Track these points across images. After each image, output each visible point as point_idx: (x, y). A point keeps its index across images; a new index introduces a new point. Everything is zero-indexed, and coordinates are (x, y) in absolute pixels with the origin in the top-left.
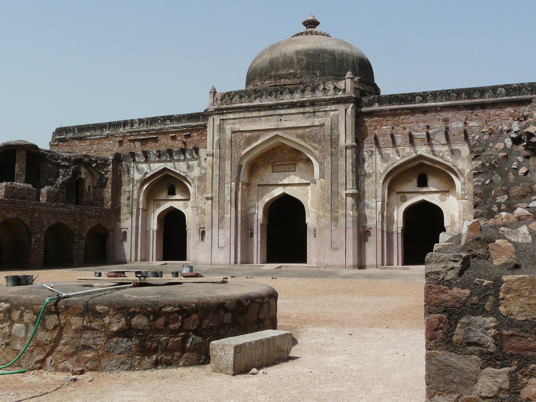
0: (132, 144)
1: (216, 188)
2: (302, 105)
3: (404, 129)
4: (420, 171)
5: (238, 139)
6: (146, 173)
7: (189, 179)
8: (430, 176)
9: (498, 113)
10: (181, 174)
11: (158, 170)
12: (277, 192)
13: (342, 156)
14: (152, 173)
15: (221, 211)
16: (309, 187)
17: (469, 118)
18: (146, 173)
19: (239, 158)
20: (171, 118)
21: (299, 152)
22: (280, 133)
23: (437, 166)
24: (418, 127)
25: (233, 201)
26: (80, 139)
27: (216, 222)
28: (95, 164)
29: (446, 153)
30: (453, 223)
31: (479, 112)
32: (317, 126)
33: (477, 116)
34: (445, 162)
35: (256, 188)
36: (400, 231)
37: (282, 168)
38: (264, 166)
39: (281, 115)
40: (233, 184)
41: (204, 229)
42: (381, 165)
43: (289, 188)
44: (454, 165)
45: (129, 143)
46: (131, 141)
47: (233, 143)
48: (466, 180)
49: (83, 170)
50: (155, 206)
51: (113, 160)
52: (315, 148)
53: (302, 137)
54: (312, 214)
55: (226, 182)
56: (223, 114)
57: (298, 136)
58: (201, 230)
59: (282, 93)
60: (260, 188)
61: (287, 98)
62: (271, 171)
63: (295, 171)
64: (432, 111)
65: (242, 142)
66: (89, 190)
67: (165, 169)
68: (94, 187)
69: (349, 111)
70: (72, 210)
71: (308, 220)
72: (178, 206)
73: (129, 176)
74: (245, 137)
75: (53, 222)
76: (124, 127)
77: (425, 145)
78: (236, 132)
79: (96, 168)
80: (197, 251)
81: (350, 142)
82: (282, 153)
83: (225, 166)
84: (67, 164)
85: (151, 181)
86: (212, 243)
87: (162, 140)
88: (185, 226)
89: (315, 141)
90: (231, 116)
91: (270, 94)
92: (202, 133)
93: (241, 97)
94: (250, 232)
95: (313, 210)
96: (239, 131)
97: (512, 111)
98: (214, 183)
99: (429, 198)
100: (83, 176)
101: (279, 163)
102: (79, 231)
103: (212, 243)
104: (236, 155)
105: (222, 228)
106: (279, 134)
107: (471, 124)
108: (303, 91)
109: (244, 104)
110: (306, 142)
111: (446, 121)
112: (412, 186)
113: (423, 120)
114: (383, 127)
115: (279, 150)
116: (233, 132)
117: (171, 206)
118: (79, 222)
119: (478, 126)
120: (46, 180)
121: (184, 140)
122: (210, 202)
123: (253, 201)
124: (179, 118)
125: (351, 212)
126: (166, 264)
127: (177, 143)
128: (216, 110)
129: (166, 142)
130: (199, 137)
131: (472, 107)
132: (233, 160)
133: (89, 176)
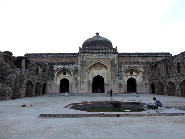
1: (81, 73)
2: (105, 53)
3: (128, 61)
6: (58, 68)
12: (97, 75)
16: (105, 74)
18: (58, 68)
20: (66, 54)
21: (103, 65)
22: (99, 60)
26: (34, 57)
30: (139, 83)
31: (145, 58)
35: (91, 73)
36: (126, 85)
39: (100, 55)
49: (39, 67)
52: (108, 64)
53: (105, 62)
56: (83, 54)
57: (104, 61)
59: (100, 50)
61: (101, 51)
69: (117, 56)
71: (105, 82)
72: (67, 78)
75: (37, 82)
76: (50, 55)
84: (35, 64)
90: (86, 54)
91: (97, 50)
93: (88, 50)
99: (133, 77)
100: (39, 68)
107: (143, 61)
108: (105, 50)
109: (89, 52)
111: (138, 59)
112: (129, 74)
116: (86, 59)
120: (30, 69)
122: (80, 77)
124: (68, 54)
128: (81, 53)
131: (144, 57)
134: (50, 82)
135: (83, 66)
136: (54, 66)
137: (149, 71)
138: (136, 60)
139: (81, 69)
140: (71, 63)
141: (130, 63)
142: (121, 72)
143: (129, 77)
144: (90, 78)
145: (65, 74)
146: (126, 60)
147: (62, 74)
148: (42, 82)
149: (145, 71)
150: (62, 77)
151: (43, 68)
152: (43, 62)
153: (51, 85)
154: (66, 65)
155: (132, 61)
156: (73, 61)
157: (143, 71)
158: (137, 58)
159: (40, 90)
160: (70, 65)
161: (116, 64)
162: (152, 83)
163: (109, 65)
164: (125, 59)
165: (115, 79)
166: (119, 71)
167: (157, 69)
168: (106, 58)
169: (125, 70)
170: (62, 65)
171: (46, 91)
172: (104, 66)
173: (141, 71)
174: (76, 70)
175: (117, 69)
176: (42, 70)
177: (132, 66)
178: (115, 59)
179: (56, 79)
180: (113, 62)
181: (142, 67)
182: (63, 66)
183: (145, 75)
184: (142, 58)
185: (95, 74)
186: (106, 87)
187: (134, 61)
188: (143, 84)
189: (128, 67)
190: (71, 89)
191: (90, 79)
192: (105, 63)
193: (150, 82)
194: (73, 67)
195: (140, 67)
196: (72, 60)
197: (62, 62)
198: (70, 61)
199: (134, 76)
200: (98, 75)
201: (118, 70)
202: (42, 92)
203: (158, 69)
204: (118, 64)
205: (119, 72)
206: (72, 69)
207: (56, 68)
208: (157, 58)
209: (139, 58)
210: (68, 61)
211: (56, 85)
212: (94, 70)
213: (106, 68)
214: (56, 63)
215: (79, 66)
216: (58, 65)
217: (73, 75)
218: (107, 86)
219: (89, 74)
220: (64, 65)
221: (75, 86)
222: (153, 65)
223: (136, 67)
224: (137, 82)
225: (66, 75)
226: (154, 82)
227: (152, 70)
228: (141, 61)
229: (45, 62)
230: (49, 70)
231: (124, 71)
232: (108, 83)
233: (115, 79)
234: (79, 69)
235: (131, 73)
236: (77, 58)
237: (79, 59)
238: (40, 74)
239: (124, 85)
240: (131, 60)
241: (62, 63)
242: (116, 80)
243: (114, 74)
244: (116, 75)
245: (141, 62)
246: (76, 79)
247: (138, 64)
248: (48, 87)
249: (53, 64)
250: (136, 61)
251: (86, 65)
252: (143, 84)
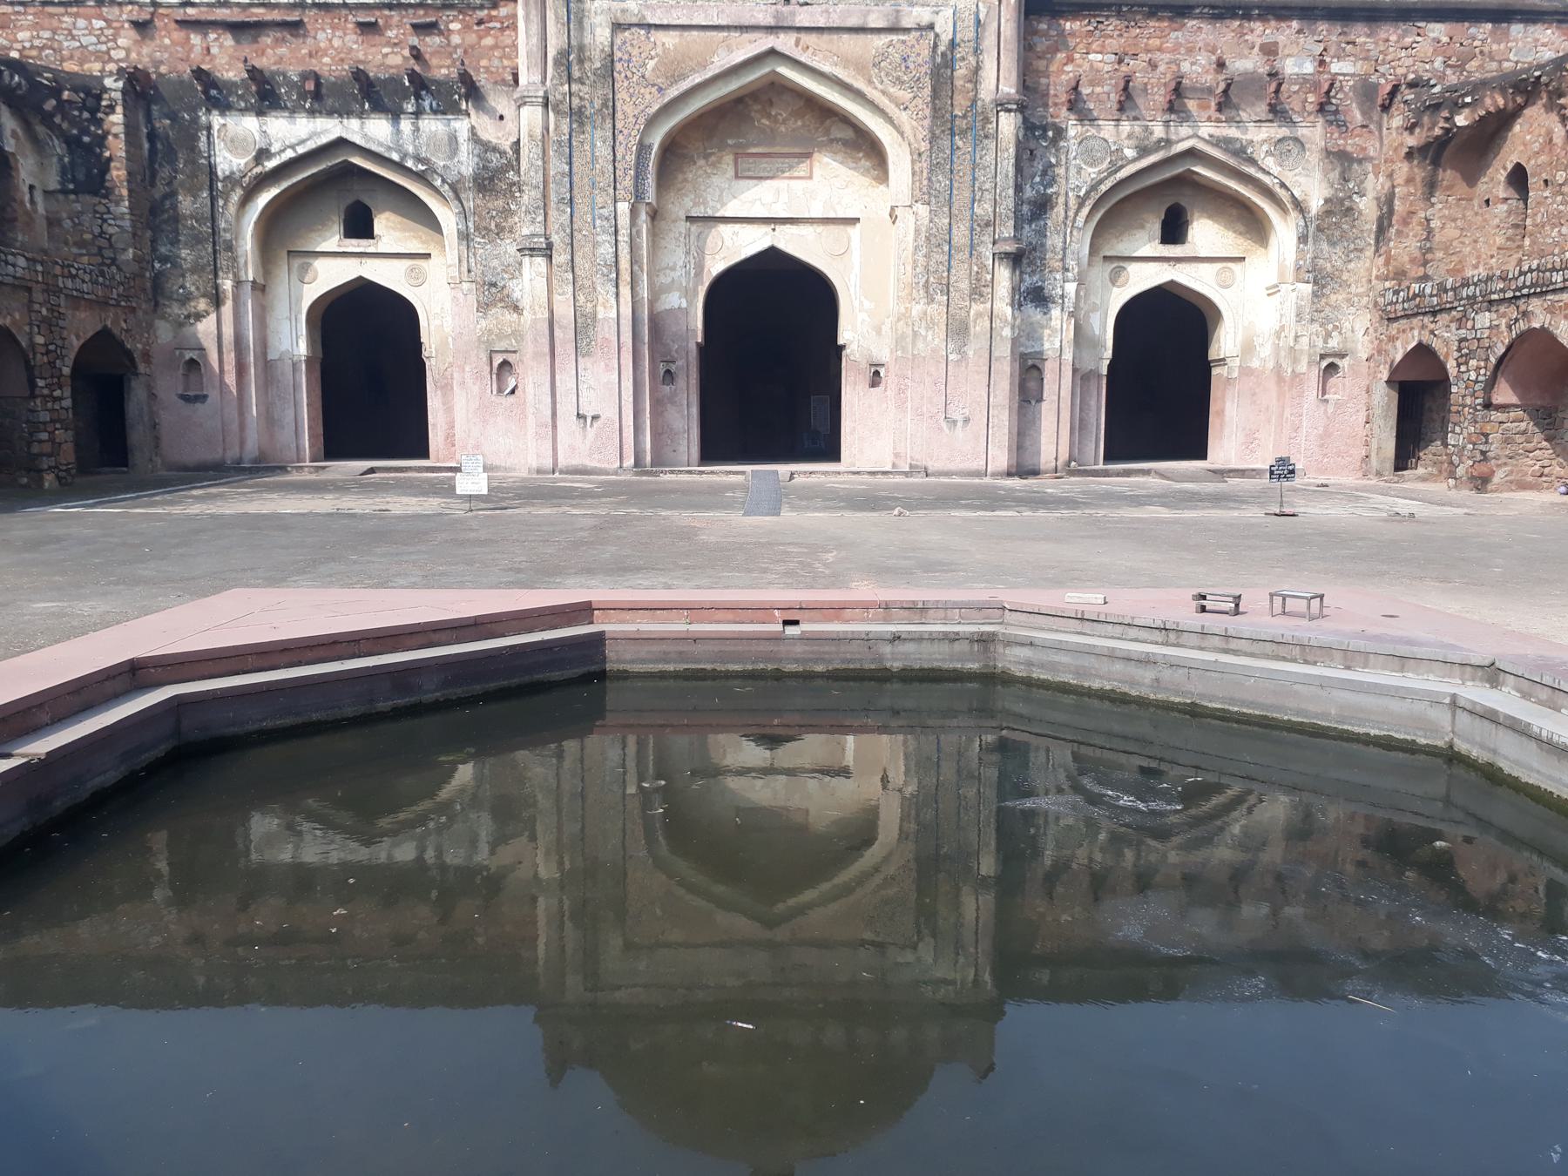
0: (196, 39)
1: (559, 218)
3: (1153, 65)
4: (1169, 198)
5: (635, 52)
6: (263, 154)
7: (438, 183)
8: (1196, 215)
9: (1408, 40)
10: (409, 164)
11: (311, 145)
13: (986, 137)
14: (290, 154)
15: (581, 299)
16: (854, 232)
17: (1332, 51)
19: (642, 120)
23: (1234, 185)
24: (1192, 64)
25: (625, 264)
27: (564, 335)
28: (53, 102)
29: (1265, 148)
30: (1248, 348)
32: (907, 30)
33: (1354, 43)
34: (1260, 176)
35: (683, 226)
36: (1105, 372)
37: (764, 164)
38: (706, 157)
40: (624, 208)
41: (511, 358)
42: (1079, 172)
43: (788, 228)
44: (1283, 185)
45: (178, 35)
46: (184, 24)
47: (618, 66)
48: (1312, 229)
50: (294, 277)
51: (124, 92)
52: (897, 105)
53: (860, 68)
54: (862, 316)
55: (599, 200)
57: (846, 62)
58: (498, 360)
60: (694, 228)
62: (731, 172)
63: (810, 177)
64: (1234, 16)
65: (651, 64)
66: (32, 201)
67: (341, 143)
68: (45, 192)
70: (20, 273)
73: (194, 162)
74: (659, 50)
77: (1209, 119)
78: (631, 25)
79: (58, 120)
80: (477, 432)
81: (1009, 89)
82: (769, 116)
83: (593, 146)
85: (285, 185)
86: (554, 403)
87: (321, 36)
88: (421, 344)
89: (899, 81)
92: (480, 22)
94: (662, 368)
95: (867, 304)
96: (640, 26)
97: (1445, 39)
98: (553, 198)
99: (1188, 277)
101: (759, 150)
102: (48, 352)
103: (554, 403)
104: (629, 109)
105: (588, 354)
106: (779, 48)
107: (1335, 67)
110: (870, 82)
111: (1270, 50)
113: (1207, 45)
114: (1091, 57)
115: (757, 107)
117: (360, 278)
118: (44, 320)
119: (1353, 75)
121: (414, 41)
122: (540, 262)
123: (673, 269)
125: (1009, 310)
126: (372, 470)
127: (386, 50)
129: (336, 43)
130: (472, 38)
132: (619, 125)
133: (28, 147)
134: (181, 325)
135: (577, 116)
136: (217, 120)
137: (1387, 203)
138: (1247, 63)
139: (557, 166)
140: (420, 84)
141: (1177, 99)
142: (1042, 206)
143: (1141, 279)
144: (664, 279)
145: (359, 225)
146: (1120, 61)
147: (322, 223)
148: (51, 325)
149: (1339, 208)
150: (332, 266)
151: (72, 143)
152: (70, 66)
153: (192, 361)
154: (361, 115)
155: (1198, 69)
156: (448, 50)
157: (1315, 204)
158: (1260, 32)
159: (36, 427)
160: (418, 114)
161: (1001, 105)
162: (1407, 356)
163: (903, 117)
164: (1114, 44)
165: (976, 293)
166: (1029, 193)
167: (1502, 176)
168: (874, 22)
169: (1093, 188)
170: (312, 113)
171: (137, 436)
172: (849, 134)
173: (1299, 206)
174: (493, 178)
175: (1008, 165)
176: (63, 171)
177: (1201, 131)
178: (989, 41)
179: (260, 288)
180: (961, 71)
181: (1313, 157)
182: (328, 129)
183: (1333, 257)
184: (1322, 27)
185: (725, 229)
186: (854, 398)
187: (1221, 65)
188: (1302, 367)
189: (1143, 151)
190: (449, 409)
191: (673, 300)
192: (859, 84)
193: (1392, 339)
194: (453, 138)
195: (1290, 146)
196: (434, 41)
197: (314, 65)
198: (417, 54)
199: (1208, 261)
200: (772, 254)
201: (1018, 188)
202: (68, 454)
203: (1518, 178)
204: (1022, 108)
205: (1025, 208)
206: (440, 164)
207: (235, 145)
208: (1517, 29)
209: (1285, 33)
210: (387, 57)
211: (267, 367)
212: (716, 180)
213: (867, 156)
214: (231, 86)
215: (532, 116)
216: (260, 113)
217: (464, 236)
218: (875, 379)
219: (654, 234)
220: (342, 112)
221: (489, 384)
222: (1461, 120)
223: (1240, 152)
224: (1225, 343)
225: (382, 247)
226: (1444, 338)
227: (1431, 186)
228: (1309, 68)
229: (94, 68)
230: (154, 174)
231: (1081, 206)
232: (883, 354)
233: (976, 293)
234: (529, 154)
235: (1174, 231)
236: (503, 11)
237: (525, 39)
238: (41, 225)
239: (1075, 371)
240: (1190, 51)
241: (317, 78)
242: (976, 308)
243: (961, 234)
244: (987, 251)
245: (1303, 80)
246: (493, 293)
247: (1262, 109)
248: (168, 386)
249: (214, 93)
250: (1250, 79)
251: (610, 108)
252: (1302, 367)
